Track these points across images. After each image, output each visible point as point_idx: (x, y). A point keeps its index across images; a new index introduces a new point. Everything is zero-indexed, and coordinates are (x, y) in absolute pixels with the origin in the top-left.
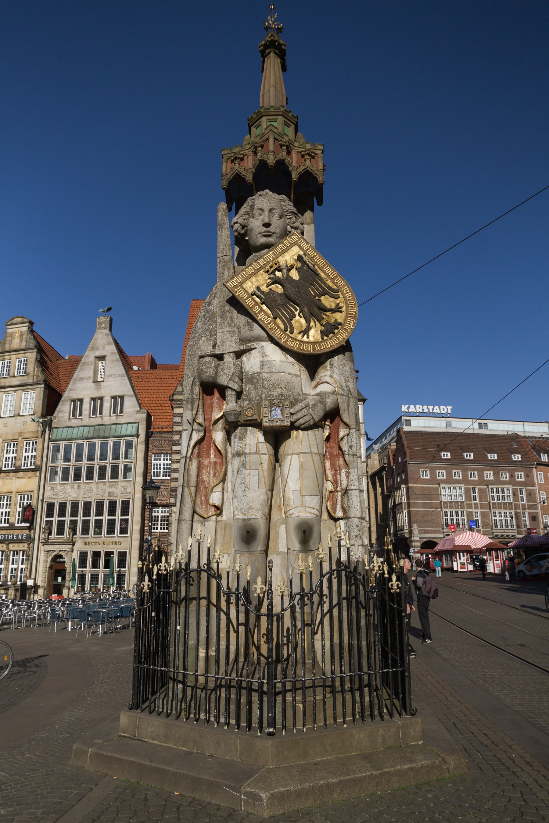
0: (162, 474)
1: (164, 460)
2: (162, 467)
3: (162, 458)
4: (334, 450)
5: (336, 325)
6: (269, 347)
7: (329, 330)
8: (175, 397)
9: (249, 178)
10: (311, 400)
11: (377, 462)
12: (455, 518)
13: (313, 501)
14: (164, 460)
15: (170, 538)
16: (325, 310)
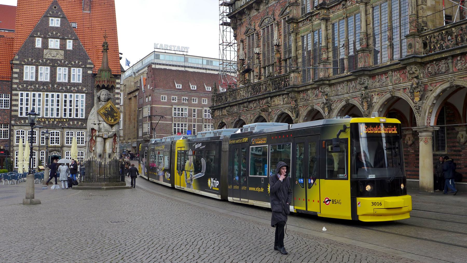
0: (3, 106)
1: (5, 97)
2: (3, 101)
3: (4, 96)
4: (115, 141)
5: (117, 119)
6: (104, 123)
7: (115, 120)
8: (14, 62)
9: (101, 87)
10: (111, 133)
11: (132, 83)
12: (180, 128)
13: (111, 150)
14: (5, 97)
15: (12, 143)
16: (114, 116)
